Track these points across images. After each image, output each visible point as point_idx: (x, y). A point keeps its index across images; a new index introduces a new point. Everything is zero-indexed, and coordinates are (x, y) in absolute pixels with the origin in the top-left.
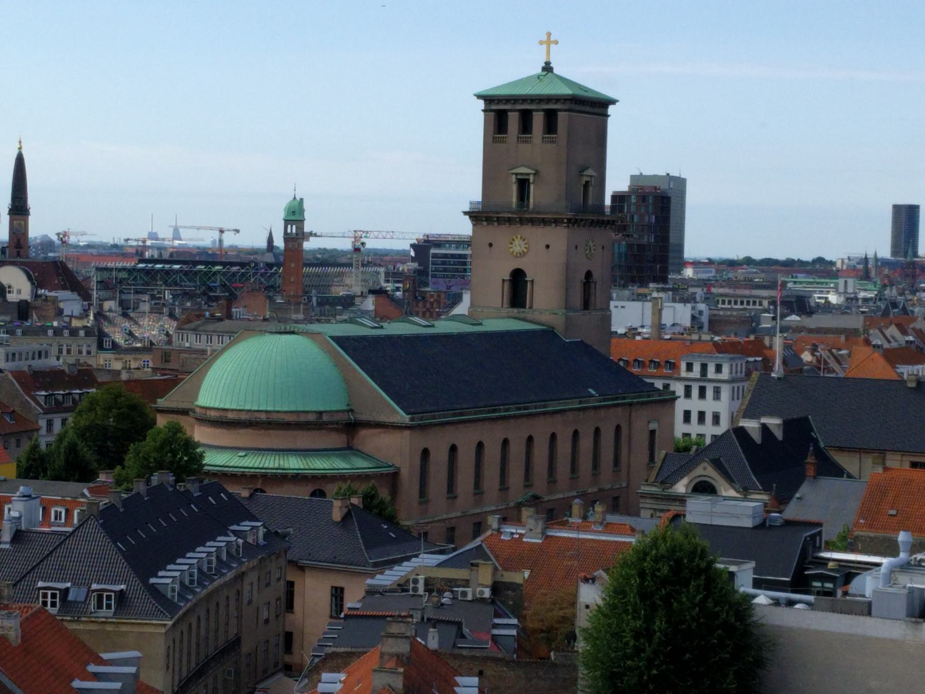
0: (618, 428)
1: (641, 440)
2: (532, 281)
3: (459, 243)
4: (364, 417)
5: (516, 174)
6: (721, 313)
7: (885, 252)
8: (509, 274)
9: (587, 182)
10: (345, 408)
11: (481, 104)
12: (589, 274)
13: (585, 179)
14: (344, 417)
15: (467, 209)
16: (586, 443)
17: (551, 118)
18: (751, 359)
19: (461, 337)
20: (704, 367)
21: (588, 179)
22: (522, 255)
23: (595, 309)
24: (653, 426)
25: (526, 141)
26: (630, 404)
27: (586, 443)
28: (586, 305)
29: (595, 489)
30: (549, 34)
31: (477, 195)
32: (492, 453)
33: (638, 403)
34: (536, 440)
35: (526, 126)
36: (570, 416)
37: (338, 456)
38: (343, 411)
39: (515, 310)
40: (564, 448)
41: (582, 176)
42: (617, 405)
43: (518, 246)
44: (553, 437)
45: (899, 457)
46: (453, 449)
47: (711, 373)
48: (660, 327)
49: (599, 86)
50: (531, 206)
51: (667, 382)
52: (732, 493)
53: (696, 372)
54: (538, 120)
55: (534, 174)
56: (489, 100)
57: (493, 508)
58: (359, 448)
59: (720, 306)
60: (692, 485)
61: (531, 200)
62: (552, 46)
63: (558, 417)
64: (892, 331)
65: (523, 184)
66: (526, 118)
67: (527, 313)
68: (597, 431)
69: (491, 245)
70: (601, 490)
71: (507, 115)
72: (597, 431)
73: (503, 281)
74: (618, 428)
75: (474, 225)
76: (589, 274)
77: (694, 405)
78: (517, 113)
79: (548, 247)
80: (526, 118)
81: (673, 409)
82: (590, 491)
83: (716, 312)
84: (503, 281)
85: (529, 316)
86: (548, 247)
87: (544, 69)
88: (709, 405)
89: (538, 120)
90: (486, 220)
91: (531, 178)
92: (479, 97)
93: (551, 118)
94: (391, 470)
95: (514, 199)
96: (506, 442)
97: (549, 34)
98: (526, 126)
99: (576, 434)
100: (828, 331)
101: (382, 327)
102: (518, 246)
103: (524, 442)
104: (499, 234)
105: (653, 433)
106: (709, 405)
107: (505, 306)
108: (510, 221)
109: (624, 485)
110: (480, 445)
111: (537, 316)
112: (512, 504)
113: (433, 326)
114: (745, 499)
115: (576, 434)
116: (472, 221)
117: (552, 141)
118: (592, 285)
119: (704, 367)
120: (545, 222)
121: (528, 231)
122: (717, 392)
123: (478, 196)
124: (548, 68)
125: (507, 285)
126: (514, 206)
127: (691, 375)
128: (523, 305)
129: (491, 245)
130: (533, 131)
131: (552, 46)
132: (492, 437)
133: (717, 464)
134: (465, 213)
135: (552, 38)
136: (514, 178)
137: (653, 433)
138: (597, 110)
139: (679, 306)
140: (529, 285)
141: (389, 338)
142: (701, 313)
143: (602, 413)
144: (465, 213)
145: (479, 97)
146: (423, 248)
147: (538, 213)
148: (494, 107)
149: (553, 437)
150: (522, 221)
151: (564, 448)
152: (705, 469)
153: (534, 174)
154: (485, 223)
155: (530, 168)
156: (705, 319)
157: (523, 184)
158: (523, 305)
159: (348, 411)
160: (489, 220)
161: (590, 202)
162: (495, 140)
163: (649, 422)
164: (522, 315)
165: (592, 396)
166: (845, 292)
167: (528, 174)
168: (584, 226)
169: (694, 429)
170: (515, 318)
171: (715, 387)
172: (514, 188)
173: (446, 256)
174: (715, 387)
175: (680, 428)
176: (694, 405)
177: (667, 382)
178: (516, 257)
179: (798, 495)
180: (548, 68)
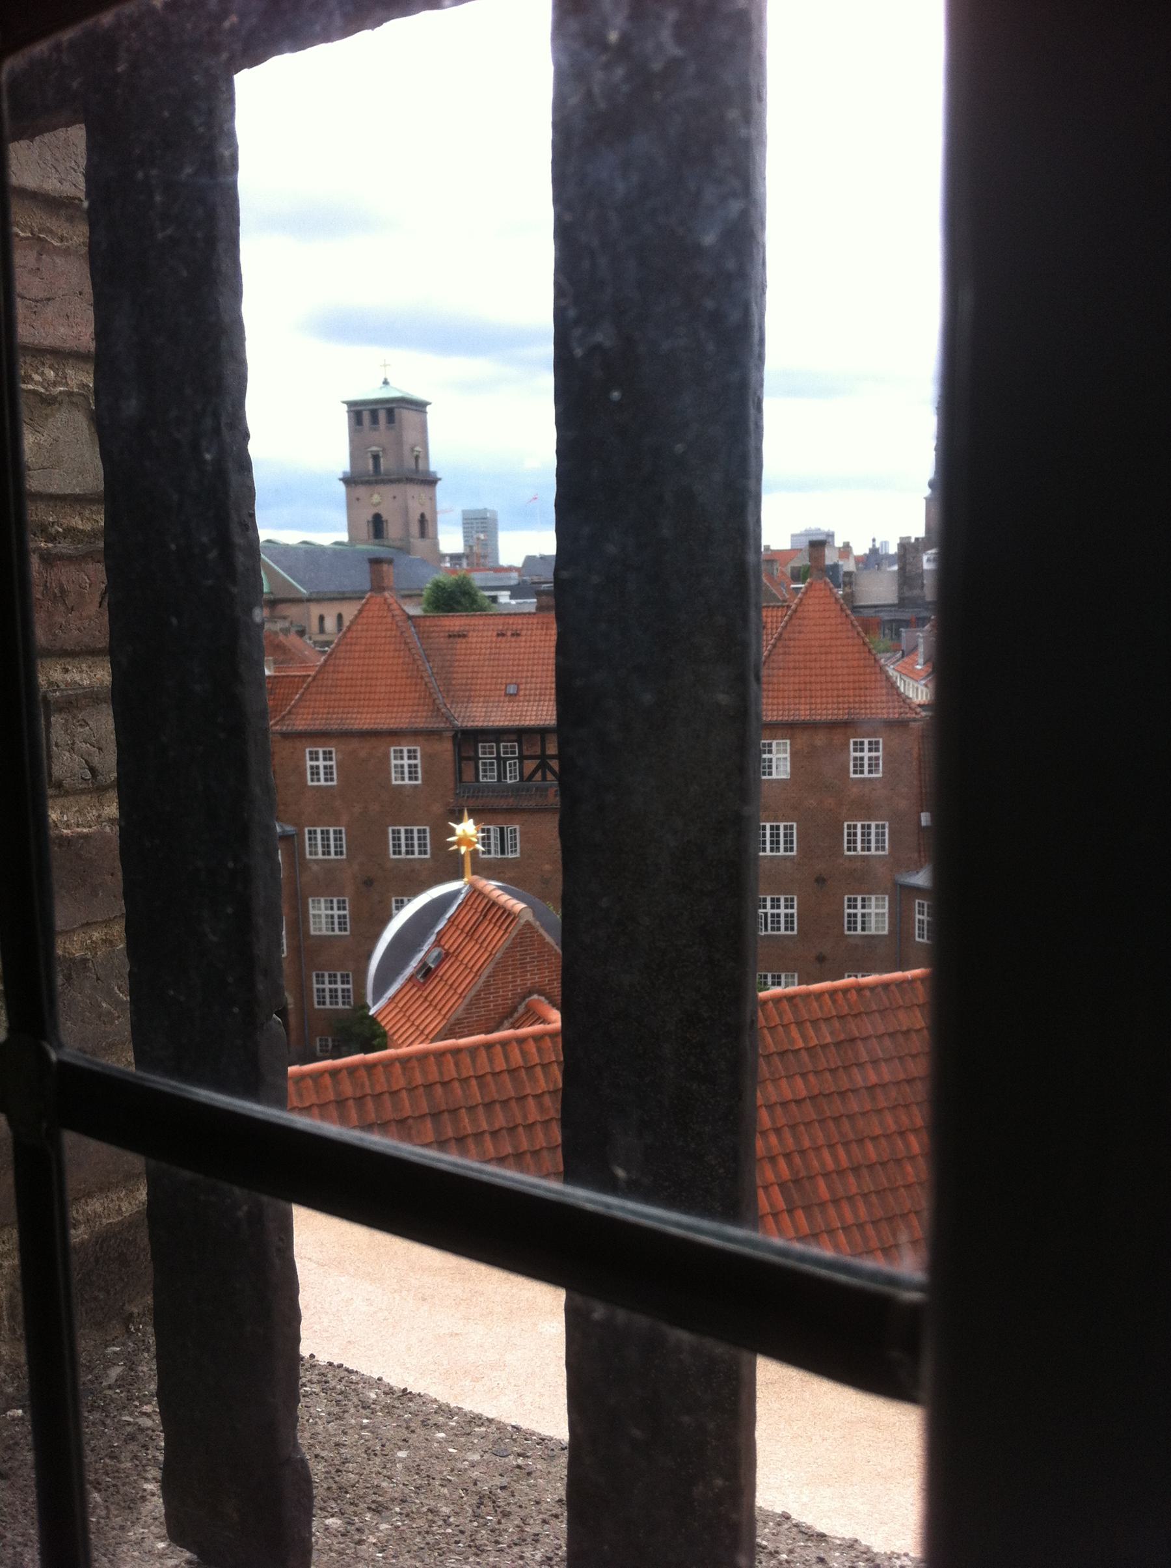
2: (387, 521)
5: (371, 451)
11: (345, 407)
12: (423, 516)
13: (415, 453)
17: (390, 413)
22: (379, 504)
23: (429, 538)
25: (375, 430)
28: (423, 534)
35: (375, 419)
39: (377, 541)
54: (382, 416)
65: (376, 458)
66: (374, 415)
75: (347, 487)
76: (423, 516)
79: (395, 497)
80: (374, 415)
84: (368, 522)
86: (395, 497)
89: (382, 416)
91: (381, 454)
92: (344, 402)
98: (375, 419)
102: (376, 498)
104: (361, 491)
107: (371, 537)
108: (368, 483)
111: (391, 543)
120: (391, 481)
125: (371, 525)
136: (369, 455)
144: (340, 479)
145: (344, 402)
150: (377, 482)
153: (382, 451)
154: (353, 485)
155: (379, 446)
157: (376, 458)
158: (383, 538)
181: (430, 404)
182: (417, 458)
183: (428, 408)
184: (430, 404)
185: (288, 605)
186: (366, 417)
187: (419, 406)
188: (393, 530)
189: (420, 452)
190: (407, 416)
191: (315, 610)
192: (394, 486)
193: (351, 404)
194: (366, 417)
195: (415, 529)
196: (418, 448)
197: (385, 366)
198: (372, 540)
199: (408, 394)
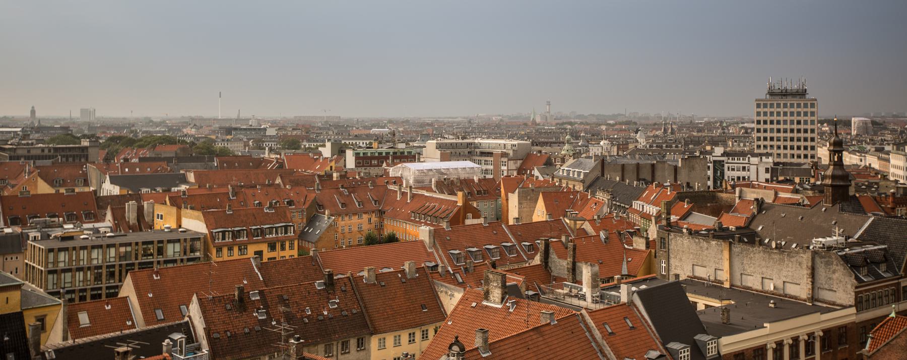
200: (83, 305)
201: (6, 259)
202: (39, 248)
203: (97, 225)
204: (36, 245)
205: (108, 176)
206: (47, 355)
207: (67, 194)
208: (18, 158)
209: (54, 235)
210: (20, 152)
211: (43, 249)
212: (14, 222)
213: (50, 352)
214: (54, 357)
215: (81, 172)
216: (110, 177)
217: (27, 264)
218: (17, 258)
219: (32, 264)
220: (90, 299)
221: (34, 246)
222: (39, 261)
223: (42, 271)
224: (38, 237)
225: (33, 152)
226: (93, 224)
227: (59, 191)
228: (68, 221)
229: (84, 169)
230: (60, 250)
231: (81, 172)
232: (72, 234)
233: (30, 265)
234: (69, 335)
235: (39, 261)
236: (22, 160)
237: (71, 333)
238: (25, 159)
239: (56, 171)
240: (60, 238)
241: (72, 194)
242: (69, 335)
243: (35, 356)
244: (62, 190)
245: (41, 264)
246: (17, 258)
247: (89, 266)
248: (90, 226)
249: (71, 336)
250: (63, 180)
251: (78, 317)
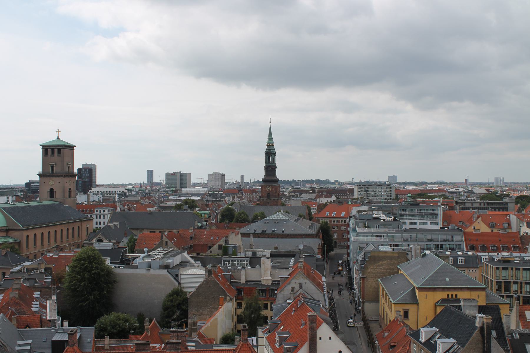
0: (79, 227)
1: (85, 230)
2: (55, 191)
3: (38, 182)
4: (11, 228)
5: (51, 165)
6: (106, 197)
7: (146, 181)
8: (49, 189)
9: (69, 166)
10: (5, 226)
11: (41, 147)
12: (70, 189)
13: (68, 165)
14: (5, 228)
15: (38, 174)
16: (71, 231)
17: (59, 150)
18: (112, 208)
19: (37, 206)
20: (100, 211)
21: (69, 165)
22: (52, 185)
23: (72, 198)
24: (87, 226)
25: (53, 156)
26: (82, 221)
27: (71, 231)
28: (70, 197)
29: (73, 243)
30: (58, 130)
31: (40, 170)
32: (46, 235)
33: (84, 221)
34: (57, 231)
35: (53, 152)
36: (66, 225)
37: (4, 238)
38: (5, 227)
39: (51, 199)
40: (65, 233)
41: (67, 165)
42: (79, 221)
43: (52, 182)
44: (62, 230)
45: (147, 230)
46: (35, 235)
47: (102, 212)
48: (88, 201)
49: (71, 142)
50: (55, 172)
51: (91, 215)
52: (107, 241)
53: (98, 212)
54: (56, 151)
55: (55, 164)
56: (43, 146)
57: (46, 249)
58: (10, 236)
59: (105, 196)
60: (97, 240)
61: (55, 171)
62: (59, 133)
63: (63, 225)
64: (147, 200)
65: (52, 167)
66: (53, 150)
67: (54, 199)
68: (73, 228)
69: (44, 182)
70: (75, 243)
71: (48, 150)
72: (73, 228)
73: (48, 191)
74: (79, 227)
76: (70, 189)
77: (98, 220)
78: (50, 149)
79: (59, 182)
80: (53, 150)
81: (93, 221)
82: (72, 243)
83: (104, 197)
85: (55, 200)
86: (59, 182)
87: (57, 138)
88: (102, 220)
89: (56, 151)
90: (43, 176)
91: (55, 166)
92: (40, 145)
93: (59, 150)
94: (18, 241)
95: (50, 171)
96: (49, 232)
97: (58, 130)
98: (53, 152)
99: (68, 229)
100: (131, 201)
101: (15, 204)
102: (52, 182)
103: (54, 232)
104: (46, 180)
105: (88, 228)
106: (102, 220)
108: (49, 176)
109: (81, 241)
110: (42, 233)
111: (57, 200)
112: (51, 248)
113: (29, 203)
114: (110, 243)
115: (68, 229)
116: (39, 176)
117: (60, 156)
118: (71, 192)
119: (100, 211)
120: (58, 176)
121: (54, 179)
122: (104, 216)
123: (41, 171)
124: (58, 138)
125: (49, 192)
126: (50, 173)
127: (97, 213)
128: (53, 197)
129: (44, 182)
130: (55, 154)
131: (59, 133)
132: (46, 231)
133: (103, 234)
134: (37, 175)
135: (59, 131)
137: (88, 228)
138: (72, 149)
139: (95, 196)
140: (55, 192)
141: (17, 207)
142: (100, 198)
143: (75, 223)
144: (37, 175)
145: (40, 145)
146: (27, 185)
147: (57, 174)
148: (44, 148)
149: (62, 230)
150: (53, 176)
151: (65, 233)
152: (100, 236)
153: (55, 164)
156: (102, 199)
157: (52, 167)
158: (53, 197)
159: (7, 226)
160: (44, 176)
161: (70, 171)
162: (45, 156)
163: (87, 225)
164: (53, 200)
165: (72, 219)
166: (136, 191)
167: (54, 164)
168: (68, 177)
169: (98, 226)
170: (52, 201)
171: (103, 216)
172: (50, 168)
173: (35, 186)
174: (103, 216)
175: (95, 226)
176: (98, 220)
177: (91, 215)
178: (51, 185)
179: (122, 241)
180: (58, 138)
181: (75, 146)
182: (69, 167)
183: (75, 148)
184: (75, 146)
185: (14, 231)
186: (50, 151)
187: (72, 147)
188: (58, 195)
189: (70, 165)
190: (65, 151)
191: (25, 233)
192: (59, 178)
193: (43, 146)
194: (50, 151)
195: (67, 194)
196: (70, 164)
197: (58, 132)
198: (49, 199)
199: (67, 143)
200: (524, 307)
201: (470, 271)
202: (491, 266)
203: (523, 255)
204: (488, 264)
205: (525, 222)
206: (514, 335)
207: (502, 233)
208: (468, 208)
209: (498, 259)
210: (467, 205)
211: (492, 267)
212: (472, 248)
213: (516, 334)
214: (519, 338)
215: (506, 219)
216: (527, 223)
217: (482, 275)
218: (475, 271)
219: (486, 276)
220: (522, 303)
221: (487, 264)
222: (490, 274)
223: (492, 280)
224: (487, 259)
225: (475, 205)
226: (520, 254)
227: (493, 230)
228: (503, 250)
229: (508, 217)
230: (503, 269)
231: (506, 219)
232: (510, 259)
233: (485, 276)
234: (520, 325)
235: (490, 274)
236: (471, 209)
237: (521, 324)
238: (473, 210)
239: (491, 217)
240: (502, 261)
241: (506, 233)
242: (520, 325)
243: (508, 335)
244: (495, 230)
245: (492, 276)
246: (475, 271)
247: (521, 281)
248: (518, 255)
249: (522, 325)
250: (495, 223)
251: (525, 314)
